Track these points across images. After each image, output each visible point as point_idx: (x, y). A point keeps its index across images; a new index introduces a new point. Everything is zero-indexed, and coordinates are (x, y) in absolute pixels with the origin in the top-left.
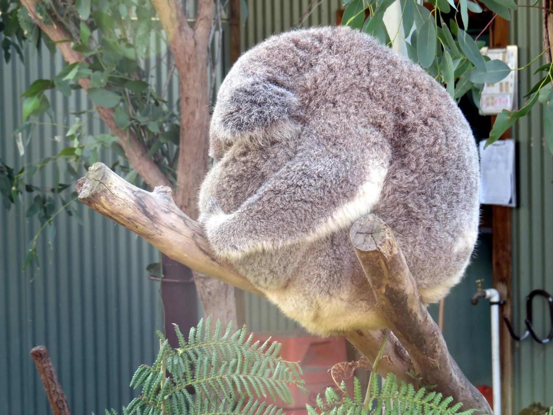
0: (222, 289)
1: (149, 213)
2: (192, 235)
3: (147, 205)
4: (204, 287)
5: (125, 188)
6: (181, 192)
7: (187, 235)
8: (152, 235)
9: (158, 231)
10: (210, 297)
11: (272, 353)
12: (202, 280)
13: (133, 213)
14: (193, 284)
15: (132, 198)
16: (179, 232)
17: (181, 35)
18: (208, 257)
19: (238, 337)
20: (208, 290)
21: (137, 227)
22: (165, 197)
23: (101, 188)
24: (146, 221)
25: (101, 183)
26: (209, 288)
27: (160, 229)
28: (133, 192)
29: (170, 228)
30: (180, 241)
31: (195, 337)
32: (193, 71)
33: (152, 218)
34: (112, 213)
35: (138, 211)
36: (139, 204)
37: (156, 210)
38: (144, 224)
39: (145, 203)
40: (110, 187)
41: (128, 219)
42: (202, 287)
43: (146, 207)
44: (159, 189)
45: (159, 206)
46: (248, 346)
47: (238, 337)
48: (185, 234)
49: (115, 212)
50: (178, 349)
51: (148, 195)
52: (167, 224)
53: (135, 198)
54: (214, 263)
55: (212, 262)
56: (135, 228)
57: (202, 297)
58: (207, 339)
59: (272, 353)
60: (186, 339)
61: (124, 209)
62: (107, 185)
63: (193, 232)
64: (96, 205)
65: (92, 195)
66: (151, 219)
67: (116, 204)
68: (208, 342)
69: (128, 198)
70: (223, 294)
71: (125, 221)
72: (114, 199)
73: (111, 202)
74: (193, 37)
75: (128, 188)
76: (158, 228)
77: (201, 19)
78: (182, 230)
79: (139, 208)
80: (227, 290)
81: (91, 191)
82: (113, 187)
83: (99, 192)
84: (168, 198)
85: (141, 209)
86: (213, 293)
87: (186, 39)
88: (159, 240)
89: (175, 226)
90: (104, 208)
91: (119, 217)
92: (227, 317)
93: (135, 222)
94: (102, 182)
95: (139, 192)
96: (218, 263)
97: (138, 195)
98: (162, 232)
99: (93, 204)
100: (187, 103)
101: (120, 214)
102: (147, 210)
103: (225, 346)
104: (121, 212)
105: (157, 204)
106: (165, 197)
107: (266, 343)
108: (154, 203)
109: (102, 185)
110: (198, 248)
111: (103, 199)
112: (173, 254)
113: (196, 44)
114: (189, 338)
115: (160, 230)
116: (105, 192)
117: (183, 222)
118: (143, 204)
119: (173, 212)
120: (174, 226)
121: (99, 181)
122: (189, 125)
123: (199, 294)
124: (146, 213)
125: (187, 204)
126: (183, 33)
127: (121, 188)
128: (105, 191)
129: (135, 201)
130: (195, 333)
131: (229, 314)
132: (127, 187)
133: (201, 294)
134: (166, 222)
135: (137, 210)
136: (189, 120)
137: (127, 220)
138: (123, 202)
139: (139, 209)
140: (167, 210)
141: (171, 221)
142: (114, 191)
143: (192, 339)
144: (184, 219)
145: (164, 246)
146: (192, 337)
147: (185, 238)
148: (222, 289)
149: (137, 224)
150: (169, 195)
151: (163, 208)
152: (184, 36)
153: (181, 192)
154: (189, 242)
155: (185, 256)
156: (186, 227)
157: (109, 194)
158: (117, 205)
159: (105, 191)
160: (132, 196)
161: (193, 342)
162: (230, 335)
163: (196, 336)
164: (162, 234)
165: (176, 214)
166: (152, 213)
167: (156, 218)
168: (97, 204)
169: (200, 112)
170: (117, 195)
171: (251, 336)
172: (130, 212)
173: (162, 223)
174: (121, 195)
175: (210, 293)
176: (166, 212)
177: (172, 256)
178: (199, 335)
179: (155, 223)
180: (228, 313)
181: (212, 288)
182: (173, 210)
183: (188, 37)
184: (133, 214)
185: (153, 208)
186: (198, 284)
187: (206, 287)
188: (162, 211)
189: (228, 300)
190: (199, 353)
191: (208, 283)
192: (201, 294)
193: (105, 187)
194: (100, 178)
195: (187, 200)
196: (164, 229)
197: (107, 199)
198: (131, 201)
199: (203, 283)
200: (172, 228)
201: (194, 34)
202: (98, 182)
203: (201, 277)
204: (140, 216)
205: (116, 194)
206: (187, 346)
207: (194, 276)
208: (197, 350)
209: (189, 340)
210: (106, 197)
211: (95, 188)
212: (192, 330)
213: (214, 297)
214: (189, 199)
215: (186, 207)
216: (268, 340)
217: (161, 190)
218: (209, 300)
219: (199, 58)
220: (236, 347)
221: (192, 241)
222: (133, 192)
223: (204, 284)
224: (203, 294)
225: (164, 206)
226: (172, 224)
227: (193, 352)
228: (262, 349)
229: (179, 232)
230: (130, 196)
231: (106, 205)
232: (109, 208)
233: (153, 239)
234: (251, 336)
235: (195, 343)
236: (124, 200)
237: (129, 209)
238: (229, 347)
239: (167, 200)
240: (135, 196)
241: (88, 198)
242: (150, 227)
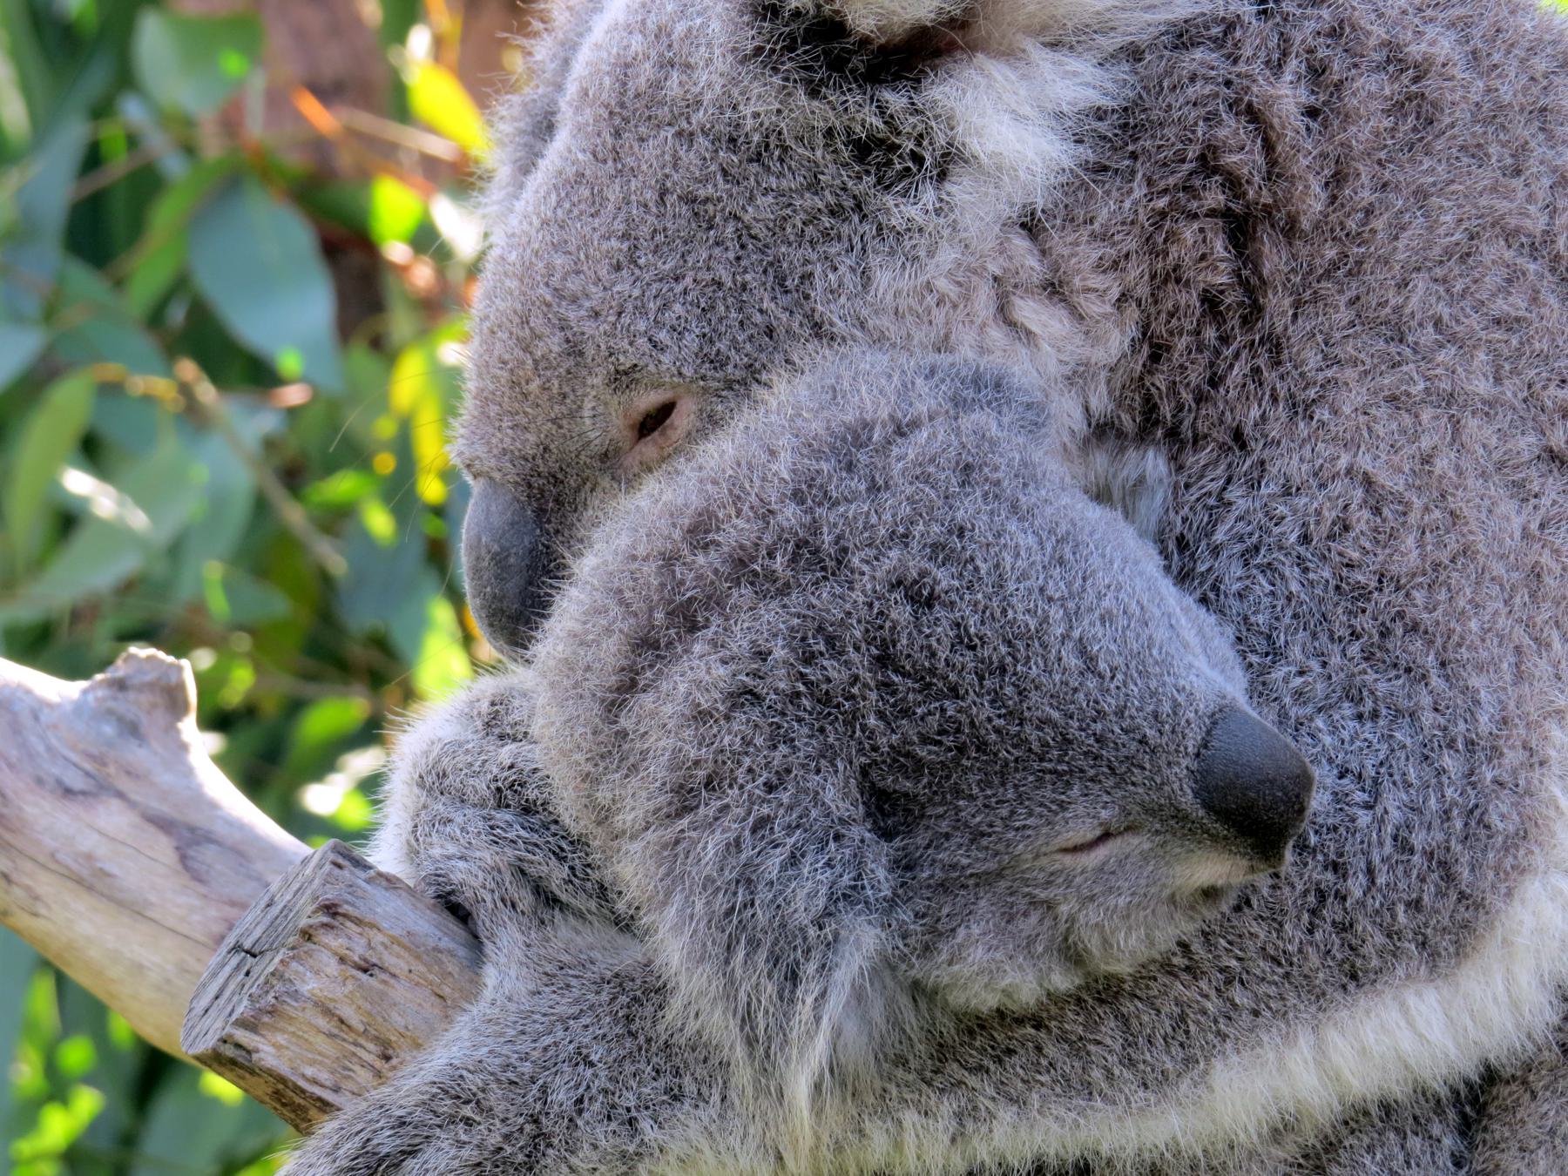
7: (183, 929)
9: (17, 891)
16: (133, 908)
22: (110, 712)
29: (79, 881)
45: (31, 756)
48: (171, 922)
52: (60, 856)
76: (14, 876)
78: (153, 898)
84: (121, 720)
89: (114, 870)
98: (37, 898)
115: (28, 889)
119: (120, 795)
134: (49, 843)
140: (76, 781)
141: (88, 842)
165: (132, 805)
176: (68, 792)
182: (124, 784)
188: (40, 781)
196: (45, 884)
225: (74, 757)
226: (89, 857)
229: (133, 908)
239: (109, 730)
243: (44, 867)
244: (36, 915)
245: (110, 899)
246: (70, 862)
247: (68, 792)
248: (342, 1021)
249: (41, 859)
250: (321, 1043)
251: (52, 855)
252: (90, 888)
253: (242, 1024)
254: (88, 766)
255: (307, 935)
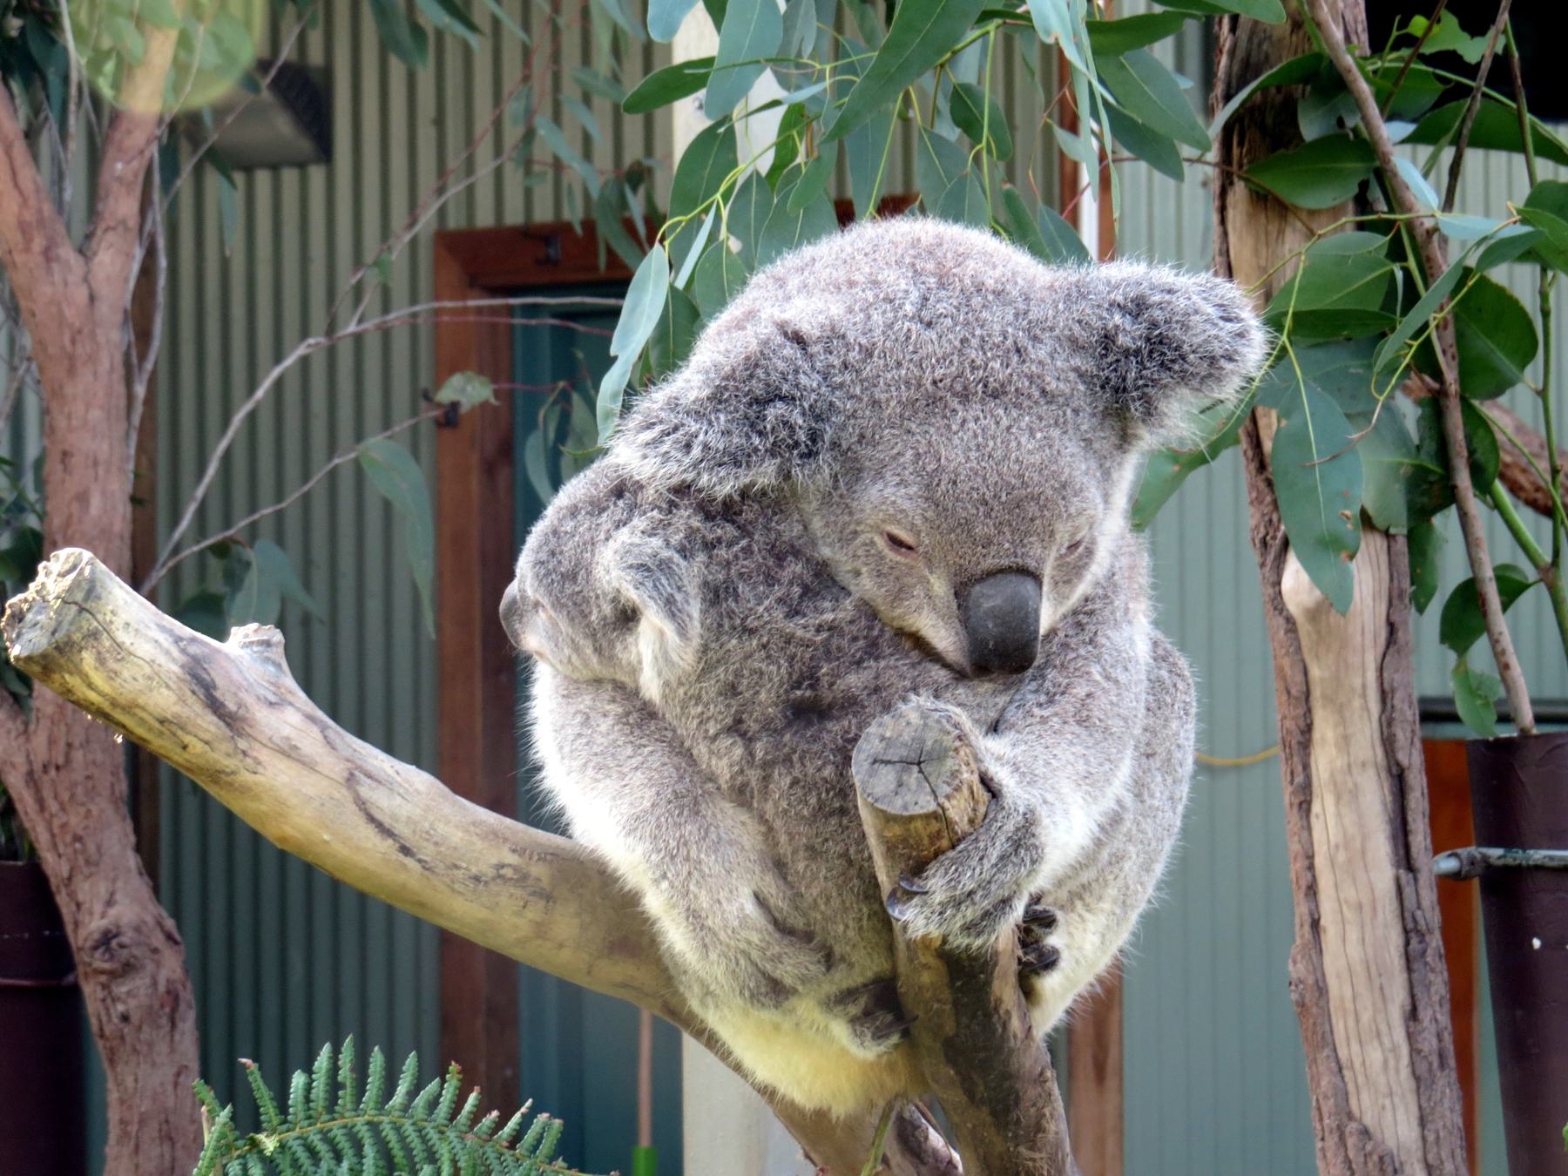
0: (162, 1006)
1: (222, 705)
2: (346, 774)
3: (219, 682)
4: (109, 1001)
5: (153, 626)
6: (45, 723)
7: (332, 775)
8: (228, 774)
9: (249, 761)
10: (126, 1030)
11: (535, 1148)
12: (103, 978)
13: (175, 704)
14: (75, 991)
15: (174, 660)
16: (308, 765)
17: (49, 271)
18: (390, 842)
19: (433, 1104)
20: (121, 1008)
21: (185, 747)
23: (84, 624)
24: (212, 729)
25: (82, 610)
26: (124, 1002)
27: (255, 754)
28: (178, 640)
30: (311, 791)
31: (308, 1100)
32: (85, 376)
33: (232, 721)
34: (114, 704)
35: (191, 699)
36: (196, 677)
37: (243, 695)
38: (207, 737)
39: (213, 674)
40: (111, 622)
41: (162, 722)
42: (104, 1000)
43: (215, 687)
44: (247, 636)
45: (251, 685)
46: (464, 1129)
47: (433, 1104)
48: (326, 772)
49: (122, 700)
50: (261, 1137)
51: (218, 651)
52: (274, 739)
53: (182, 659)
54: (409, 861)
55: (401, 857)
56: (179, 750)
57: (101, 1029)
58: (344, 1106)
59: (535, 1148)
60: (283, 1108)
61: (151, 690)
62: (100, 617)
63: (349, 765)
64: (67, 676)
65: (57, 648)
66: (228, 725)
67: (126, 674)
68: (347, 1114)
69: (162, 659)
70: (164, 1021)
71: (150, 729)
72: (123, 659)
73: (111, 670)
74: (86, 280)
75: (162, 628)
76: (249, 752)
77: (108, 229)
79: (196, 688)
80: (174, 1010)
81: (53, 633)
82: (118, 622)
83: (77, 637)
85: (201, 692)
86: (135, 1018)
87: (66, 284)
88: (249, 789)
89: (299, 745)
90: (90, 686)
91: (134, 715)
92: (176, 1085)
93: (180, 733)
94: (88, 607)
95: (193, 640)
96: (420, 861)
97: (193, 649)
98: (259, 763)
99: (56, 677)
100: (66, 469)
101: (138, 706)
102: (217, 694)
103: (397, 1129)
104: (141, 701)
105: (246, 679)
106: (267, 659)
107: (517, 1117)
108: (236, 676)
109: (88, 615)
110: (362, 814)
111: (88, 659)
112: (288, 830)
113: (92, 298)
114: (290, 1102)
115: (255, 759)
116: (96, 639)
117: (319, 737)
118: (205, 676)
119: (291, 704)
120: (295, 748)
121: (76, 603)
122: (70, 532)
123: (94, 1021)
124: (215, 706)
125: (61, 761)
126: (55, 266)
127: (141, 627)
128: (94, 635)
129: (182, 667)
130: (308, 1088)
131: (182, 1079)
132: (158, 625)
133: (100, 1021)
134: (270, 733)
135: (189, 693)
136: (70, 516)
137: (157, 725)
138: (148, 670)
139: (193, 692)
140: (273, 699)
141: (287, 731)
142: (121, 636)
143: (300, 1107)
144: (324, 729)
145: (263, 808)
146: (301, 1099)
147: (325, 782)
148: (162, 1006)
149: (187, 739)
150: (278, 654)
151: (262, 692)
152: (57, 278)
153: (45, 723)
154: (337, 795)
155: (326, 837)
156: (328, 748)
157: (107, 643)
158: (130, 679)
159: (94, 635)
160: (175, 652)
161: (301, 1115)
162: (413, 1094)
163: (313, 1096)
164: (260, 769)
165: (298, 709)
166: (231, 706)
167: (244, 720)
168: (71, 673)
169: (104, 493)
170: (132, 649)
171: (472, 1099)
172: (164, 700)
173: (260, 738)
174: (144, 649)
175: (125, 1018)
176: (271, 704)
177: (284, 839)
178: (322, 1095)
179: (240, 735)
180: (178, 1074)
181: (132, 1003)
183: (71, 279)
184: (177, 709)
185: (233, 689)
186: (91, 991)
187: (115, 1000)
188: (258, 698)
189: (177, 1037)
190: (322, 1148)
191: (121, 989)
192: (100, 1021)
193: (95, 624)
194: (79, 597)
195: (62, 746)
196: (264, 755)
197: (101, 660)
198: (172, 667)
199: (104, 987)
200: (289, 752)
201: (88, 272)
202: (74, 608)
203: (103, 972)
204: (197, 715)
205: (128, 643)
206: (285, 1127)
207: (81, 969)
208: (315, 1139)
209: (291, 1110)
210: (99, 653)
211: (65, 625)
212: (298, 1080)
213: (139, 1029)
214: (69, 745)
215: (58, 768)
216: (523, 1110)
217: (255, 638)
218: (122, 1038)
219: (101, 339)
220: (432, 1131)
221: (344, 791)
222: (178, 640)
223: (110, 993)
224: (104, 1019)
226: (288, 739)
227: (304, 1145)
228: (505, 1136)
229: (308, 765)
230: (167, 653)
231: (98, 678)
232: (106, 688)
233: (231, 784)
234: (472, 1099)
235: (309, 1117)
236: (151, 663)
237: (164, 691)
238: (409, 1129)
239: (272, 669)
240: (183, 651)
241: (44, 656)
242: (226, 747)
243: (265, 746)
244: (255, 773)
245: (298, 761)
246: (279, 742)
247: (271, 704)
248: (972, 792)
249: (265, 741)
250: (963, 802)
251: (270, 739)
252: (289, 756)
253: (948, 797)
254: (272, 688)
255: (956, 750)
